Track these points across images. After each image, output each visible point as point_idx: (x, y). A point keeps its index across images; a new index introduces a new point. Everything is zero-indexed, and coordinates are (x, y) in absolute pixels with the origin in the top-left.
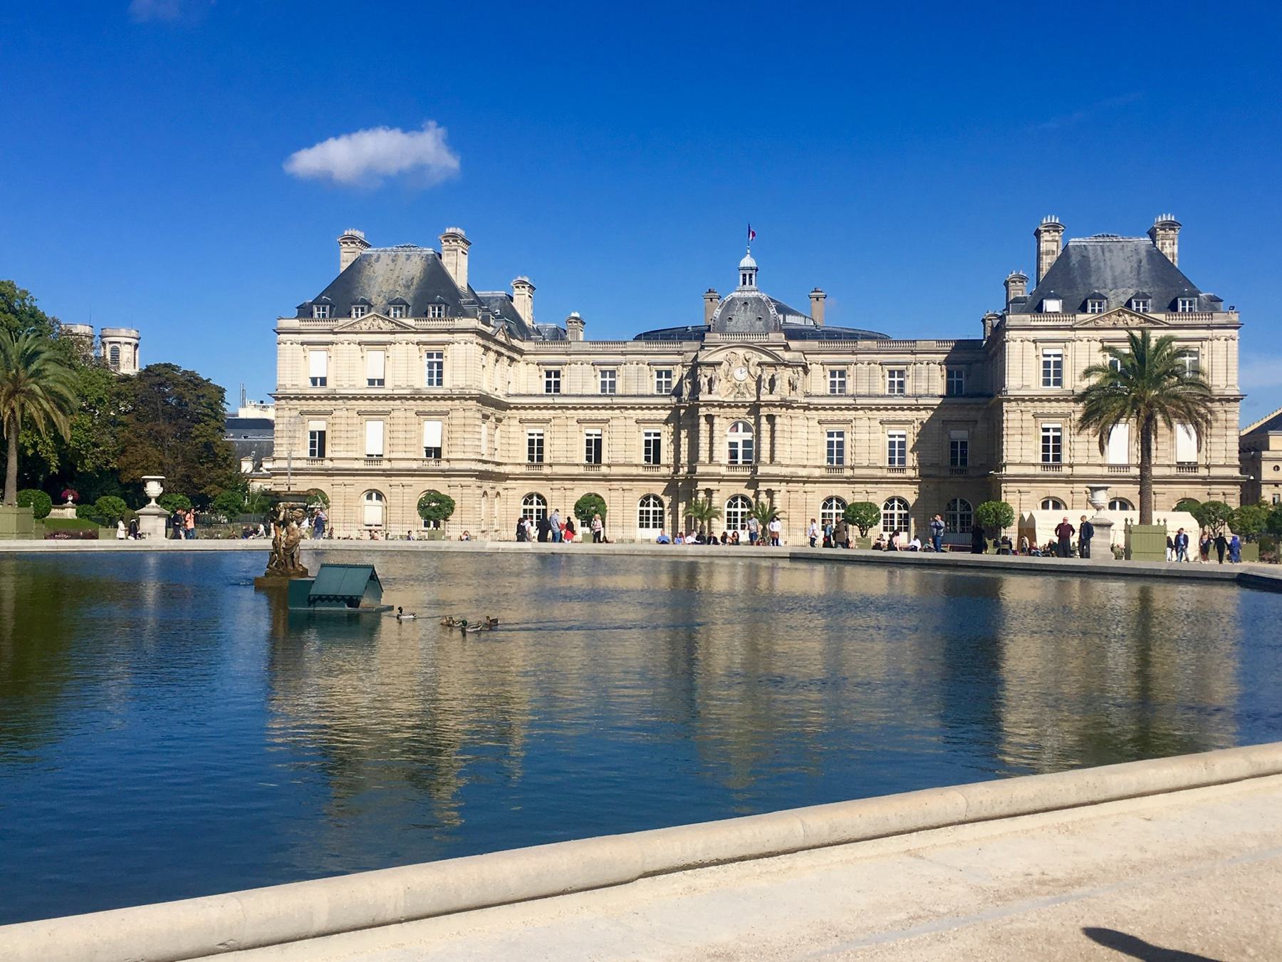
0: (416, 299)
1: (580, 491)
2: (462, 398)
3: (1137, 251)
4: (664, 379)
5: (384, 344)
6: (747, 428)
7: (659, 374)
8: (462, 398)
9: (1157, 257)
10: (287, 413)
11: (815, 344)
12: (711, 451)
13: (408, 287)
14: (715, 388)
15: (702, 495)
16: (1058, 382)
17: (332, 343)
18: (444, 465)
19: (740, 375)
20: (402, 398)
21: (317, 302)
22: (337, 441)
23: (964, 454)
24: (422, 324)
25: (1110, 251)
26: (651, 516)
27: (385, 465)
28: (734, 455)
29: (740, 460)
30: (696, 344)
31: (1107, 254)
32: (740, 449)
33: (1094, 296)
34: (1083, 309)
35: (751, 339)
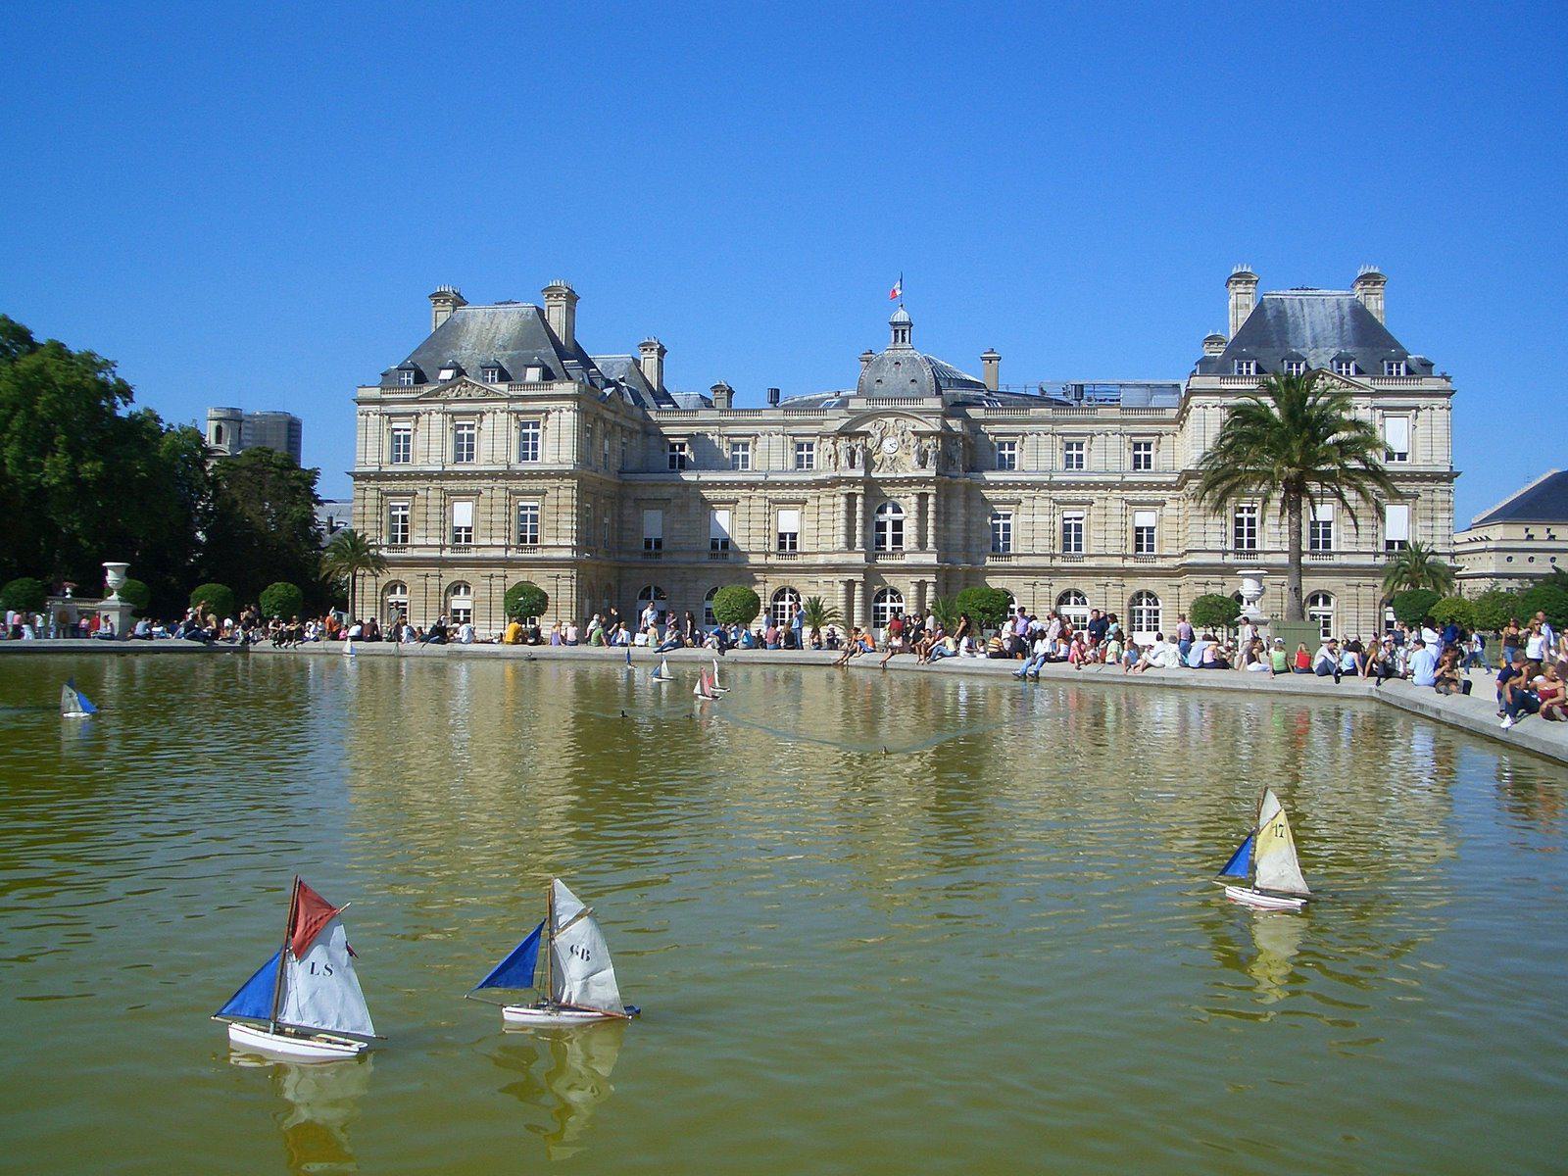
4: (805, 453)
5: (474, 413)
6: (897, 510)
7: (800, 447)
8: (560, 475)
9: (1360, 313)
13: (505, 348)
15: (842, 587)
17: (418, 415)
20: (493, 475)
22: (423, 525)
25: (1311, 306)
26: (787, 612)
27: (473, 553)
29: (889, 547)
30: (842, 412)
31: (1306, 310)
32: (889, 533)
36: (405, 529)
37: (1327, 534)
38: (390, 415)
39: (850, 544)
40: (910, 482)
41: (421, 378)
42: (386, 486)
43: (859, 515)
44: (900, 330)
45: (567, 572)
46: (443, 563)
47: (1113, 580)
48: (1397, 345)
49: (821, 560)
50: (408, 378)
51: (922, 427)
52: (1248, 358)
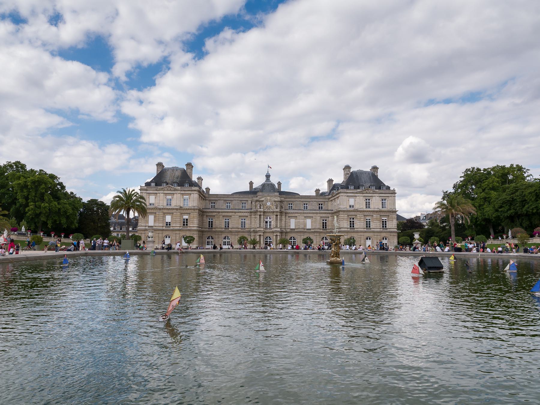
0: (180, 181)
3: (369, 174)
8: (194, 209)
11: (285, 196)
12: (260, 224)
14: (262, 207)
18: (188, 228)
19: (269, 204)
20: (177, 209)
21: (152, 182)
24: (183, 188)
27: (171, 228)
34: (359, 189)
37: (370, 224)
38: (149, 193)
39: (260, 227)
40: (274, 212)
41: (156, 185)
43: (262, 219)
45: (195, 233)
46: (163, 230)
47: (318, 234)
49: (252, 230)
50: (153, 184)
51: (276, 200)
52: (352, 185)
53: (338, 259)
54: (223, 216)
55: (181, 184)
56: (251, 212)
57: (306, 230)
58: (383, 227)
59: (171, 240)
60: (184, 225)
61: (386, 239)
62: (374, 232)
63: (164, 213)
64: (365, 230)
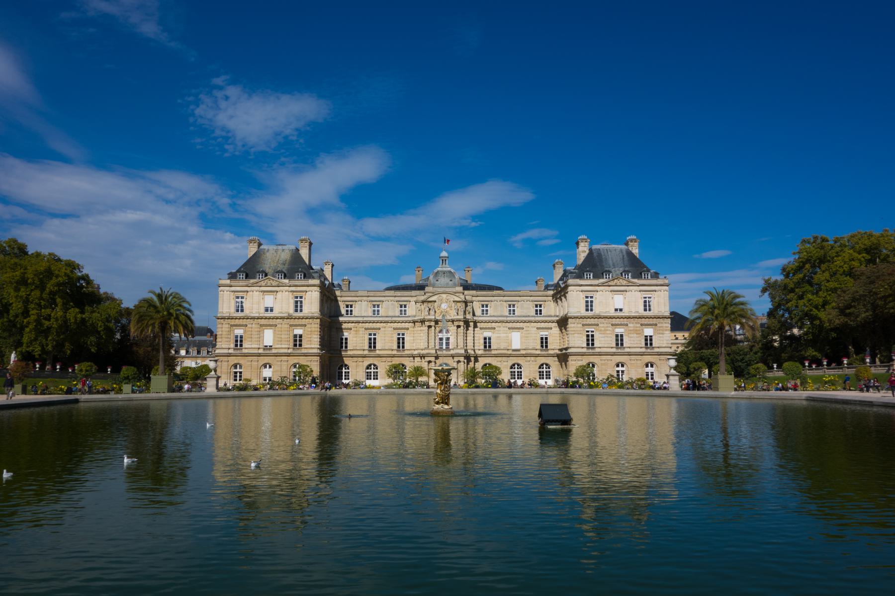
0: (288, 270)
1: (367, 362)
2: (312, 318)
3: (621, 250)
7: (401, 306)
8: (312, 318)
9: (630, 254)
10: (224, 326)
11: (474, 292)
14: (432, 312)
16: (592, 310)
18: (304, 351)
19: (444, 306)
21: (239, 271)
23: (546, 342)
27: (274, 351)
28: (441, 344)
30: (422, 292)
32: (444, 341)
33: (606, 271)
35: (447, 290)
36: (241, 341)
37: (622, 340)
40: (453, 321)
41: (247, 277)
42: (233, 322)
44: (444, 260)
46: (259, 355)
48: (644, 266)
49: (416, 352)
50: (242, 276)
52: (590, 271)
53: (446, 407)
54: (366, 329)
55: (289, 274)
56: (414, 322)
57: (510, 352)
58: (646, 344)
59: (273, 372)
60: (295, 345)
61: (652, 366)
62: (629, 354)
63: (261, 326)
64: (614, 350)
